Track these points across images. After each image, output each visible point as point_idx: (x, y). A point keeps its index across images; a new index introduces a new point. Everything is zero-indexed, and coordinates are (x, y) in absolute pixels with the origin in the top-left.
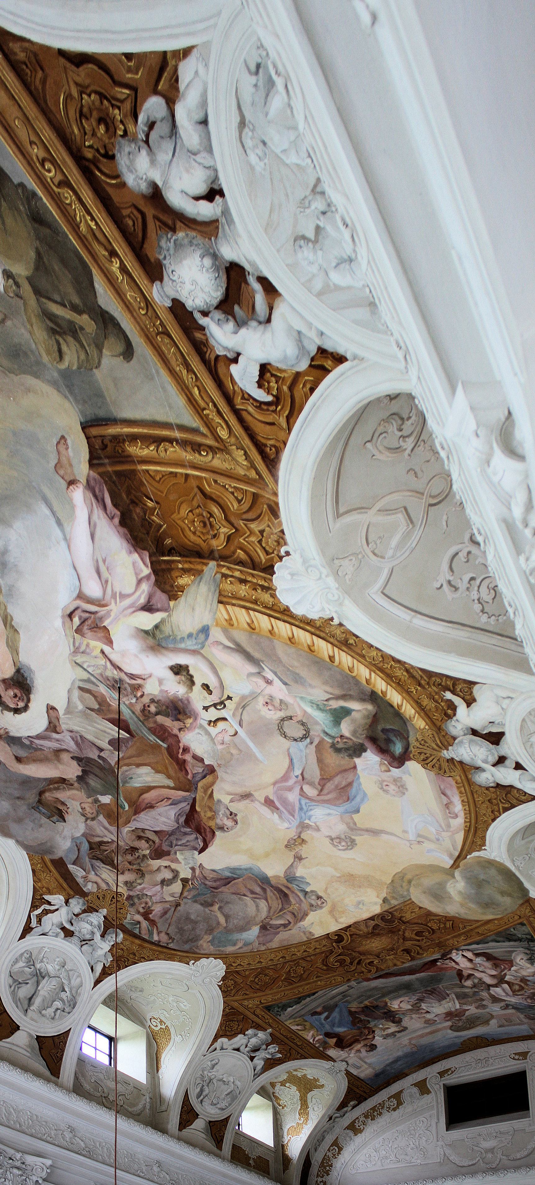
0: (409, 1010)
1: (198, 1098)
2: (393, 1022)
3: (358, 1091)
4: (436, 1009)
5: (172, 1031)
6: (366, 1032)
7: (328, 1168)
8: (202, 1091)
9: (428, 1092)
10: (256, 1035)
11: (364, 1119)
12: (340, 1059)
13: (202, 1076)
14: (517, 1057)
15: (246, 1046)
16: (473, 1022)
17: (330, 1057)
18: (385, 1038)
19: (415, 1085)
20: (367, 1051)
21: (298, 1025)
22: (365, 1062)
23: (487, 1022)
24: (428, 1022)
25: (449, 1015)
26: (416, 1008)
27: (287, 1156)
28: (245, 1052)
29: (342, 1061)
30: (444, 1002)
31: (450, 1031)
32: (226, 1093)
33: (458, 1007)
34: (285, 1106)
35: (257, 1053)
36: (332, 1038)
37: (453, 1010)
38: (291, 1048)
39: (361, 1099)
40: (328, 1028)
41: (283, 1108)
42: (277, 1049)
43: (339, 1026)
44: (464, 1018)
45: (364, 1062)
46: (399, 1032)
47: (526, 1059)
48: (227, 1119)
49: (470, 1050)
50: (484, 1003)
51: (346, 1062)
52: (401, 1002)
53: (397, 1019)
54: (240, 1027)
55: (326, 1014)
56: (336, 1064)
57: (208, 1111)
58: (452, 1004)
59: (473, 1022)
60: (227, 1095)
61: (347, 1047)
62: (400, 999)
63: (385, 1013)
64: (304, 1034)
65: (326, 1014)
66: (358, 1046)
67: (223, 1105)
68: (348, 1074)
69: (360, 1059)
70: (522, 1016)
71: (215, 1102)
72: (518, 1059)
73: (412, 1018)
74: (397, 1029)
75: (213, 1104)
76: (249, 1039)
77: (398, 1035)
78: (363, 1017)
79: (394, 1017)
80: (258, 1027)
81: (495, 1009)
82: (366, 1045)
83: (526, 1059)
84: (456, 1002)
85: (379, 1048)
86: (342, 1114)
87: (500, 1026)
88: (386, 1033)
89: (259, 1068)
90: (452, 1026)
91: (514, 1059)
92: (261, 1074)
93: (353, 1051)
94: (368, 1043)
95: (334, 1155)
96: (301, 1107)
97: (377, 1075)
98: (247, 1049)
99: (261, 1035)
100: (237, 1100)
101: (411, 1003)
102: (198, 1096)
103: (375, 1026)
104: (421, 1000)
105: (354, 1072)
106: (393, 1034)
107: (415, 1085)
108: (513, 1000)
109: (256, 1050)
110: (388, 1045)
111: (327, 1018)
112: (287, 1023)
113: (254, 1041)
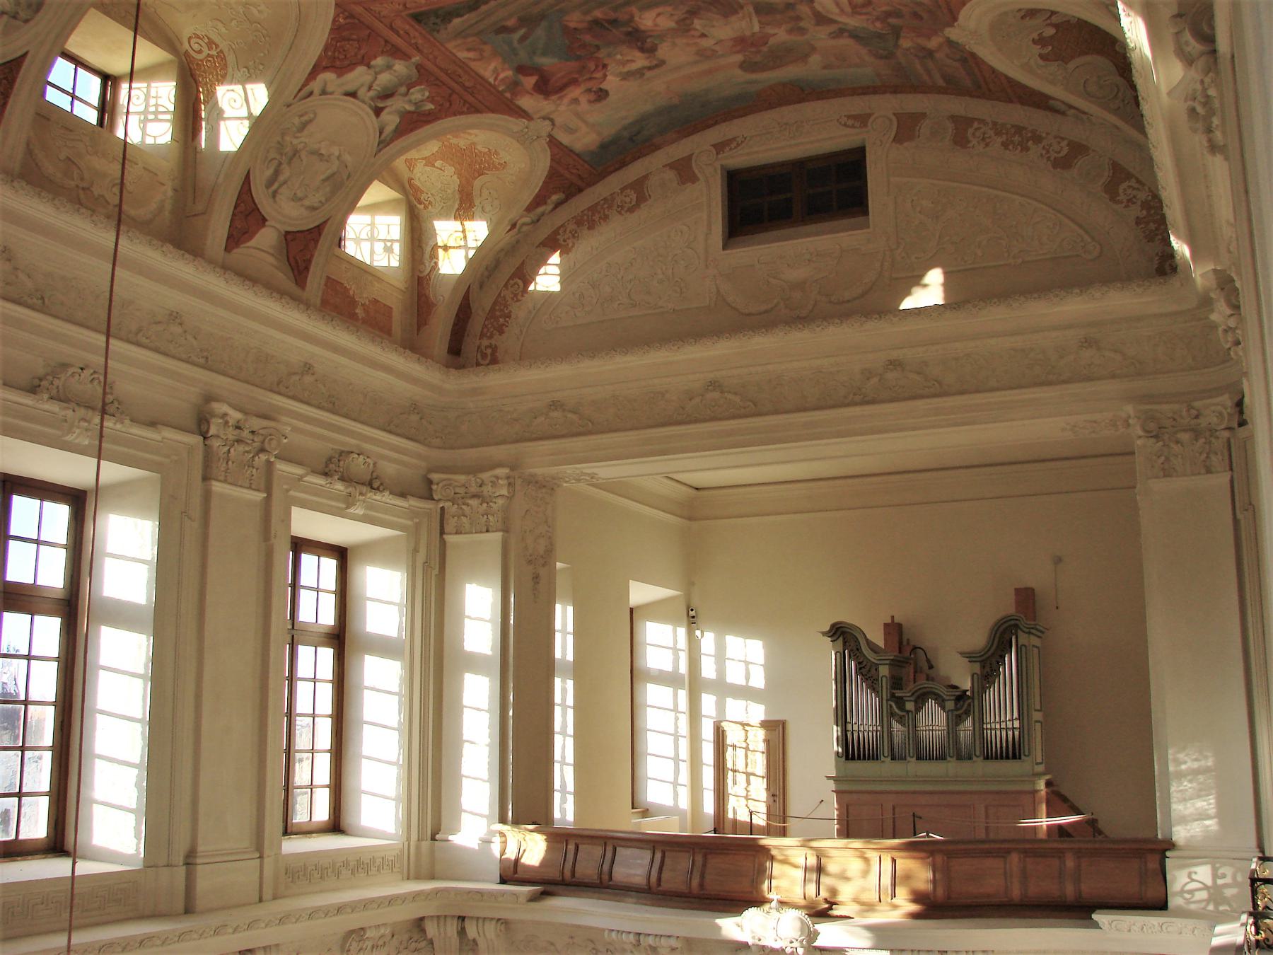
0: (673, 29)
1: (268, 187)
2: (642, 50)
3: (567, 175)
4: (722, 30)
5: (231, 59)
6: (592, 66)
7: (502, 320)
8: (277, 173)
9: (693, 179)
10: (389, 67)
11: (574, 227)
12: (543, 114)
13: (281, 145)
14: (850, 122)
15: (370, 88)
16: (780, 56)
17: (524, 111)
18: (624, 79)
19: (671, 166)
20: (590, 102)
21: (469, 50)
22: (585, 122)
23: (804, 58)
24: (704, 55)
25: (741, 42)
26: (684, 27)
27: (427, 297)
28: (367, 99)
29: (544, 118)
30: (733, 18)
31: (739, 72)
32: (323, 177)
33: (756, 28)
34: (430, 203)
35: (389, 102)
36: (531, 75)
37: (748, 33)
38: (455, 96)
39: (572, 191)
40: (523, 57)
41: (426, 207)
42: (427, 94)
43: (544, 54)
44: (765, 49)
45: (582, 122)
46: (650, 68)
47: (865, 126)
48: (319, 230)
49: (771, 106)
50: (802, 24)
51: (552, 121)
52: (659, 15)
53: (648, 45)
54: (362, 52)
55: (522, 32)
56: (532, 124)
57: (286, 212)
58: (746, 24)
59: (780, 56)
60: (324, 181)
61: (557, 92)
62: (660, 10)
63: (629, 34)
64: (479, 67)
65: (522, 32)
66: (575, 92)
67: (313, 200)
68: (553, 142)
69: (577, 115)
70: (864, 51)
71: (300, 194)
72: (853, 127)
73: (674, 45)
74: (646, 63)
75: (295, 199)
76: (377, 73)
77: (648, 74)
78: (587, 38)
79: (644, 42)
80: (396, 53)
81: (820, 36)
82: (589, 90)
83: (865, 126)
84: (755, 20)
85: (613, 97)
86: (535, 218)
87: (825, 68)
88: (626, 70)
89: (389, 129)
90: (744, 62)
91: (845, 125)
92: (392, 140)
93: (566, 101)
94: (593, 85)
95: (516, 295)
96: (461, 205)
97: (604, 147)
98: (372, 93)
99: (400, 67)
100: (345, 194)
101: (676, 18)
102: (270, 183)
103: (609, 55)
104: (693, 13)
105: (564, 139)
106: (640, 73)
107: (671, 166)
108: (853, 22)
109: (387, 95)
110: (629, 90)
111: (523, 39)
112: (450, 46)
113: (385, 78)
